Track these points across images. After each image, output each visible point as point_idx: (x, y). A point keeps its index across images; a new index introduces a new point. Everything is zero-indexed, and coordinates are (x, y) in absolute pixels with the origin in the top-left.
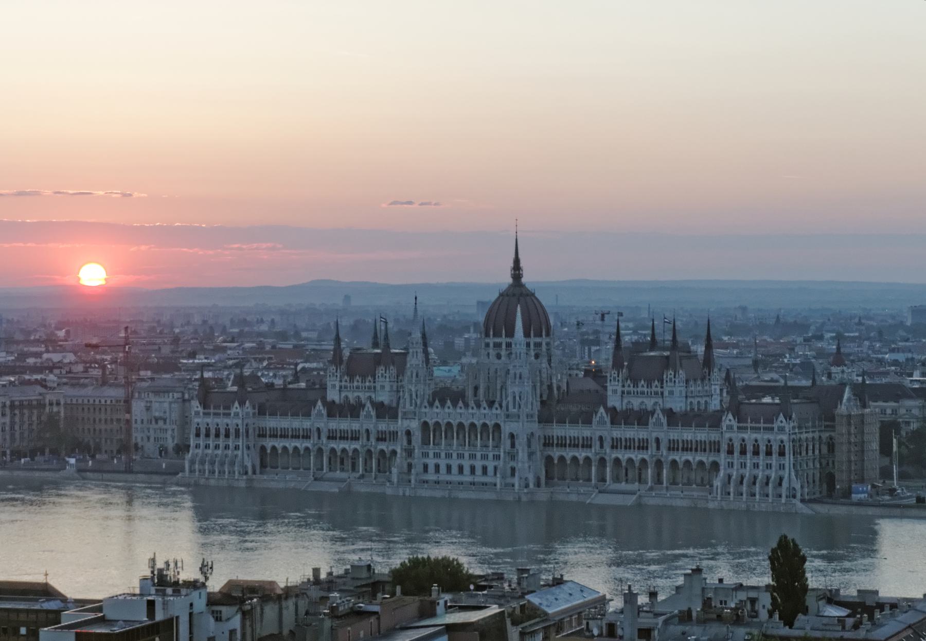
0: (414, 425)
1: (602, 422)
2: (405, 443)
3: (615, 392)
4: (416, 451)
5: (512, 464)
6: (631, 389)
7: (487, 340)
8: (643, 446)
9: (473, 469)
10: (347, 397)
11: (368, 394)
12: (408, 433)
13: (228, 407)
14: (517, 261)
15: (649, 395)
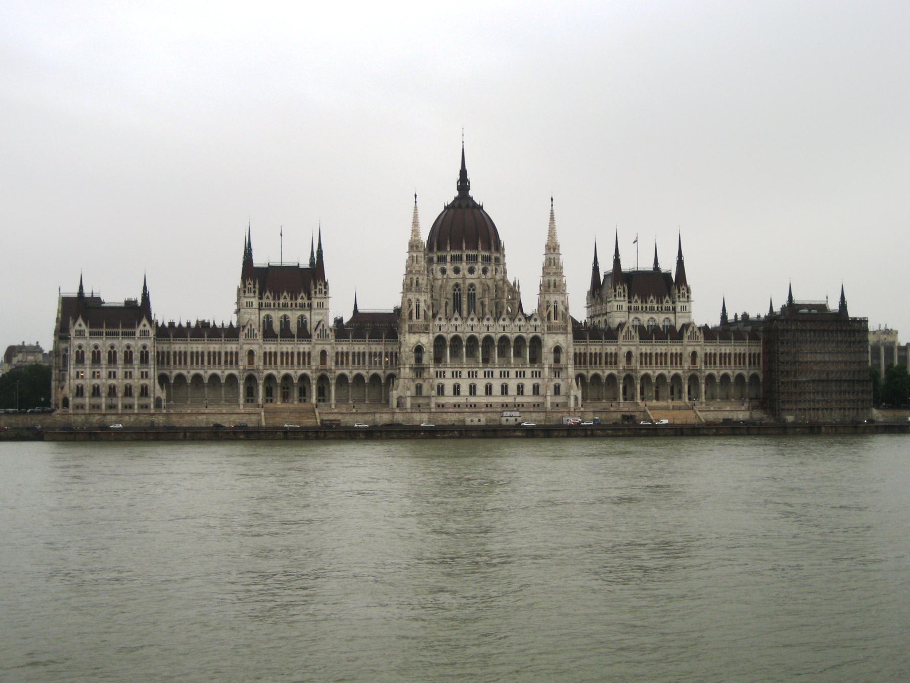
0: (426, 340)
1: (628, 337)
2: (413, 361)
3: (620, 308)
4: (432, 370)
5: (557, 381)
6: (639, 304)
7: (458, 253)
8: (677, 358)
9: (504, 390)
10: (268, 316)
11: (299, 313)
12: (419, 349)
13: (133, 326)
14: (463, 172)
15: (661, 311)
